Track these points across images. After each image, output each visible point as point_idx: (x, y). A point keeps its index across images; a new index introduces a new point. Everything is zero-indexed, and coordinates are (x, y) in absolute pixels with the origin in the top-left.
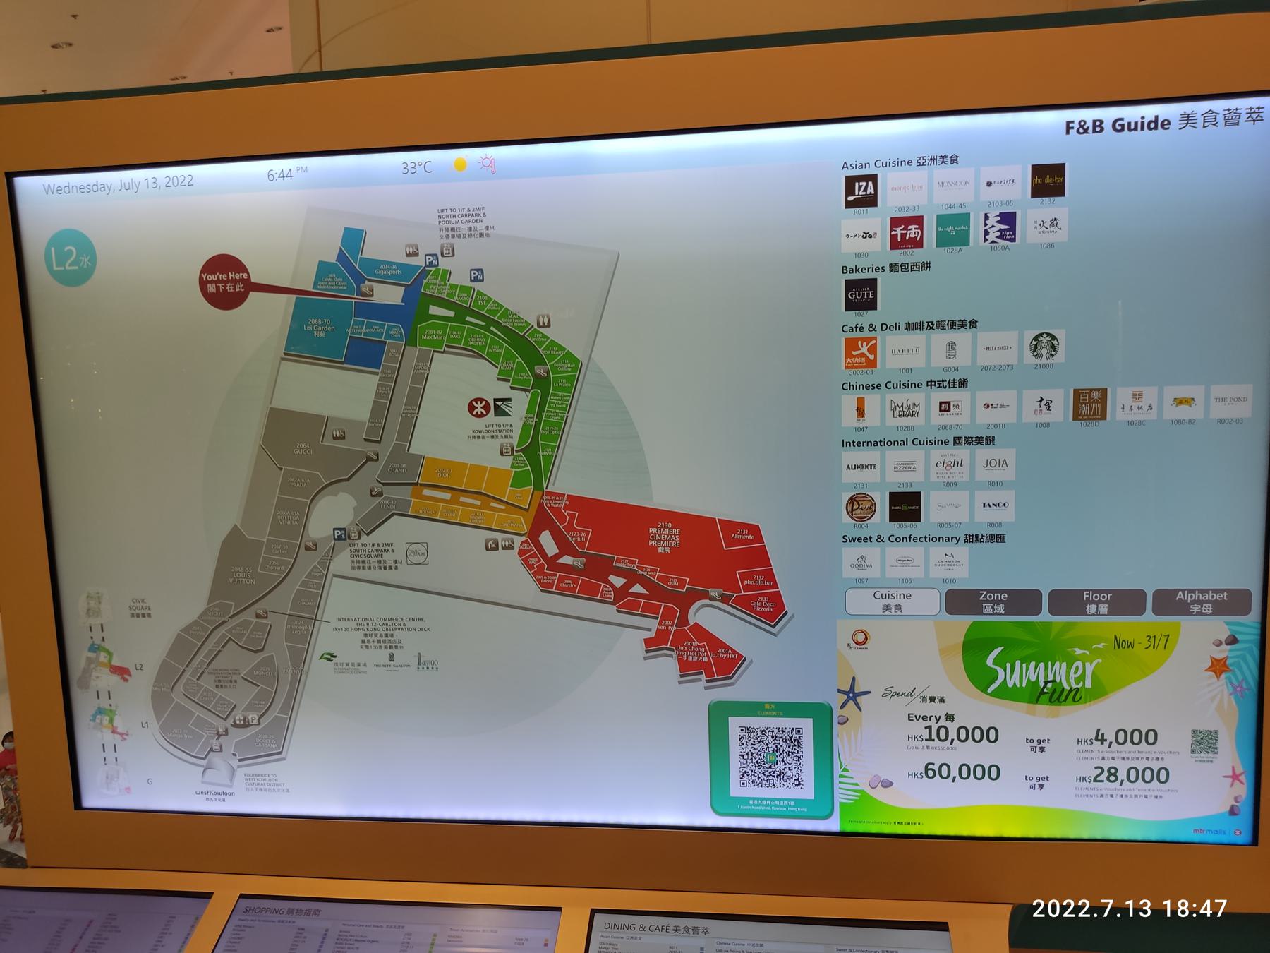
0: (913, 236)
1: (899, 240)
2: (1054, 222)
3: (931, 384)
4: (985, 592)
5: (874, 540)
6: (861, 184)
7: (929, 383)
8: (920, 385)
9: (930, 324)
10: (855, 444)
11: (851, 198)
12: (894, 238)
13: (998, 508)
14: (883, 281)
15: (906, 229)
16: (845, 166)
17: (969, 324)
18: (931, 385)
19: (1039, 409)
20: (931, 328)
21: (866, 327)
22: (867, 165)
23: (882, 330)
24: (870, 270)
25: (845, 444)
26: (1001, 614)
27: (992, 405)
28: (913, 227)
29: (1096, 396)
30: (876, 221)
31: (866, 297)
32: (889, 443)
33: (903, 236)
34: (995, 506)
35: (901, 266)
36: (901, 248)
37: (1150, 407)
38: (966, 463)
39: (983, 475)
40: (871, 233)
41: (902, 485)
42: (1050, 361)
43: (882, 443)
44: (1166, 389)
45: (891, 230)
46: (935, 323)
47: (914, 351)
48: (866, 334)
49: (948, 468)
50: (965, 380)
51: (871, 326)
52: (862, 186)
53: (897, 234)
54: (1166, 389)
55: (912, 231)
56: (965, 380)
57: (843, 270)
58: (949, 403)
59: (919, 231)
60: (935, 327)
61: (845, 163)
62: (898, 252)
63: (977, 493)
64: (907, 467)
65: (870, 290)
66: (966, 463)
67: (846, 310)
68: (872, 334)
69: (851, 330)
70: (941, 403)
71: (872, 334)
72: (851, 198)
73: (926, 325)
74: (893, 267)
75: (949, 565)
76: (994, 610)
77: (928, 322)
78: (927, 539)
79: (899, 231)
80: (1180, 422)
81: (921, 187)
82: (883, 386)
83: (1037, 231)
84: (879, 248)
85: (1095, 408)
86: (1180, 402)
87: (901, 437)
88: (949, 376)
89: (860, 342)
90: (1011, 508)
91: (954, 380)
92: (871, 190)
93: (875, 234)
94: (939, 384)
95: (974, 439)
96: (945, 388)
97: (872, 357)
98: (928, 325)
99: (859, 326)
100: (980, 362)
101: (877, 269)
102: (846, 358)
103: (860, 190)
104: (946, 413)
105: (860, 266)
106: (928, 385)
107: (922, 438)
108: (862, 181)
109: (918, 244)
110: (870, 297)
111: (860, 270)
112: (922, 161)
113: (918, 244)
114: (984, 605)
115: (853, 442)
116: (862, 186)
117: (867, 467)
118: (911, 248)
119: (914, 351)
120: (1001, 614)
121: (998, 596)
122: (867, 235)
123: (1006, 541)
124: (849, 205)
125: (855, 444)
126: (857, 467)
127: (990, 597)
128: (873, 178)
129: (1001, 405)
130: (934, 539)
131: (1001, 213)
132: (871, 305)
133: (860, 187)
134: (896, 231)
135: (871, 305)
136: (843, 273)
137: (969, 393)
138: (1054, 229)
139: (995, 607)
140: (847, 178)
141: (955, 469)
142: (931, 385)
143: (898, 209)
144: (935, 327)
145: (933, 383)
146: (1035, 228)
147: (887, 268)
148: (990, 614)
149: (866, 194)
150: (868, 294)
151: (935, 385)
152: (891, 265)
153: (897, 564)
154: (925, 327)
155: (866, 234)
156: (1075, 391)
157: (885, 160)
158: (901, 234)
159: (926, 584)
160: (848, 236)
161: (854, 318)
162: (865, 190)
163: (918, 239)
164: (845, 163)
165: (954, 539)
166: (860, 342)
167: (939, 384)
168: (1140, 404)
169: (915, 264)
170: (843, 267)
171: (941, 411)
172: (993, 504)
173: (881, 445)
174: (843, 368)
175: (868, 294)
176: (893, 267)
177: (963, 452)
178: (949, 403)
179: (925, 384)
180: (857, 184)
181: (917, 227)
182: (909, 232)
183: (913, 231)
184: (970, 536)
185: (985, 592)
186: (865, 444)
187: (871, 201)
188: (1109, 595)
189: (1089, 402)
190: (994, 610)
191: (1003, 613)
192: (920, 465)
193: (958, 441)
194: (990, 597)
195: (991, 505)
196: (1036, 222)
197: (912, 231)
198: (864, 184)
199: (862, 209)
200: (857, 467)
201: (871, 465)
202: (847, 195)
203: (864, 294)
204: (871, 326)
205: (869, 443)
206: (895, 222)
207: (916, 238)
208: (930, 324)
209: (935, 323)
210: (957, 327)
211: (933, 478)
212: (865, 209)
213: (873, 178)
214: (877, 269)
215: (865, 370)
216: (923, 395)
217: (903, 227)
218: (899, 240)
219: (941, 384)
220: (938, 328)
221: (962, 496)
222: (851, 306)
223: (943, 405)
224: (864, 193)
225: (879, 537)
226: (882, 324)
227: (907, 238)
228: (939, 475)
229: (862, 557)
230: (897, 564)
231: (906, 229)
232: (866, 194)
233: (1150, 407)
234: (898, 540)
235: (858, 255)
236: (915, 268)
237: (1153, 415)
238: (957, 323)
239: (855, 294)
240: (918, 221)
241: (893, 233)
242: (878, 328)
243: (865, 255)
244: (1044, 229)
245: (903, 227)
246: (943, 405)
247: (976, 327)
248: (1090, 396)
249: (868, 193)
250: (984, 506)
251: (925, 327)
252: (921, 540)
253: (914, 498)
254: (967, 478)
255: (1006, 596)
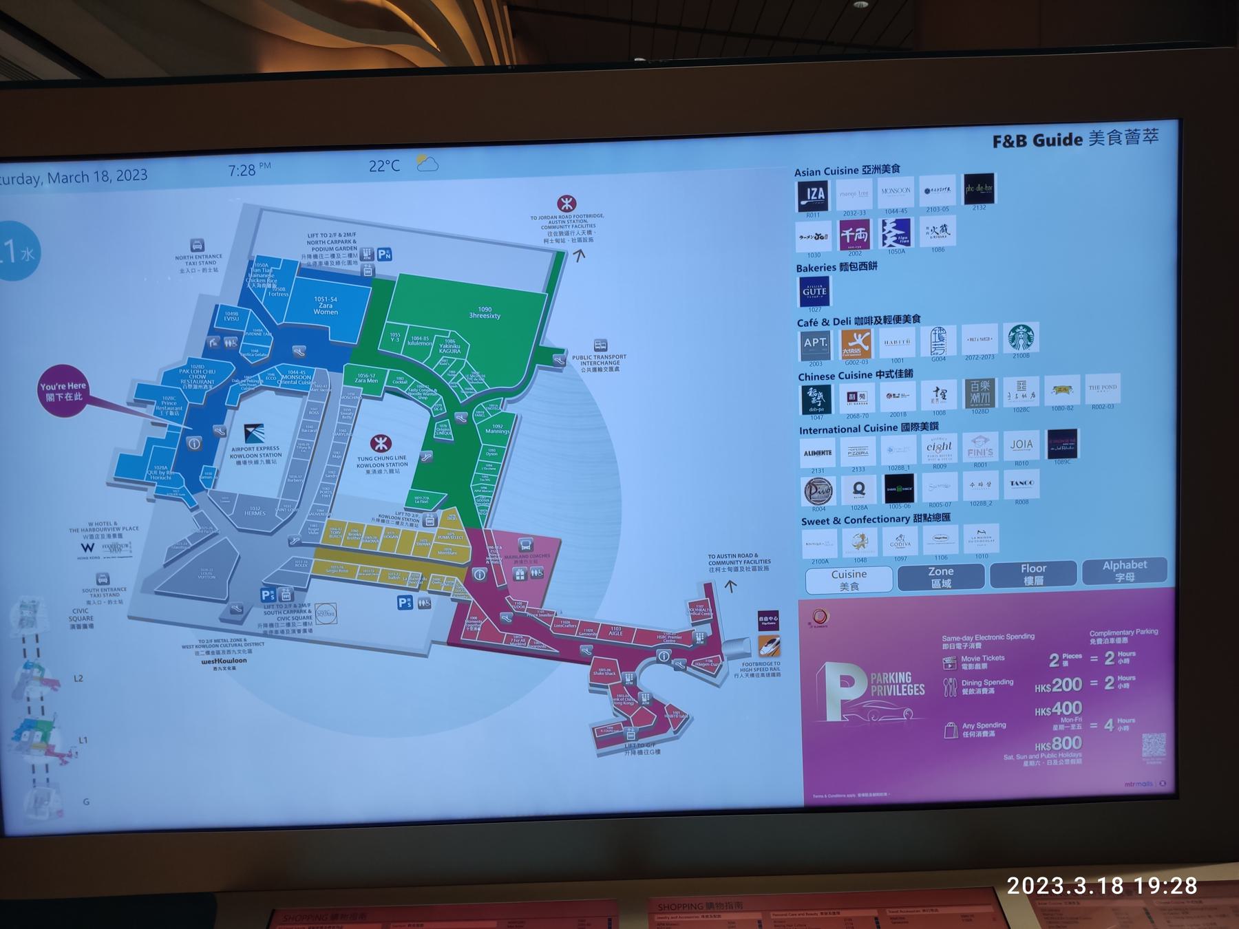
0: (860, 238)
1: (848, 241)
2: (944, 228)
3: (880, 374)
4: (933, 568)
5: (831, 521)
6: (813, 189)
7: (878, 374)
8: (870, 375)
9: (878, 318)
10: (812, 431)
11: (803, 203)
12: (843, 239)
13: (1024, 486)
14: (835, 279)
15: (854, 231)
16: (798, 173)
17: (912, 319)
18: (880, 375)
19: (935, 398)
20: (879, 323)
21: (820, 321)
22: (818, 173)
23: (835, 324)
24: (823, 269)
25: (802, 431)
26: (949, 589)
27: (894, 395)
28: (861, 229)
29: (985, 386)
30: (825, 224)
31: (819, 293)
32: (843, 430)
33: (852, 237)
34: (1023, 484)
35: (851, 265)
36: (850, 249)
37: (1033, 395)
38: (954, 446)
39: (1011, 456)
40: (823, 235)
41: (815, 471)
42: (1027, 351)
43: (837, 431)
44: (1047, 378)
45: (841, 232)
46: (882, 318)
47: (905, 342)
48: (820, 328)
49: (938, 451)
50: (911, 371)
51: (824, 320)
52: (813, 191)
53: (846, 236)
54: (1047, 378)
55: (860, 234)
56: (911, 371)
57: (798, 268)
58: (856, 393)
59: (866, 233)
60: (882, 322)
61: (798, 170)
62: (847, 252)
63: (965, 473)
64: (861, 452)
65: (823, 287)
66: (954, 446)
67: (801, 306)
68: (826, 328)
69: (806, 324)
70: (849, 394)
71: (826, 328)
72: (803, 203)
73: (874, 320)
74: (844, 267)
75: (981, 541)
76: (942, 585)
77: (876, 317)
78: (880, 520)
79: (847, 233)
80: (1059, 408)
81: (867, 193)
82: (837, 376)
83: (929, 236)
84: (829, 250)
85: (985, 397)
86: (1059, 390)
87: (853, 424)
88: (896, 367)
89: (855, 334)
90: (1037, 485)
91: (901, 370)
92: (821, 195)
93: (826, 235)
94: (888, 374)
95: (920, 425)
96: (893, 378)
97: (866, 348)
98: (876, 320)
99: (813, 321)
100: (965, 352)
101: (828, 268)
102: (843, 349)
103: (813, 195)
104: (853, 403)
105: (813, 265)
106: (877, 376)
107: (873, 425)
108: (814, 187)
109: (865, 245)
110: (823, 293)
111: (813, 269)
112: (867, 170)
113: (865, 245)
114: (933, 580)
115: (810, 429)
116: (813, 191)
117: (823, 453)
118: (859, 249)
119: (905, 342)
120: (949, 589)
121: (945, 572)
122: (819, 237)
123: (951, 519)
124: (802, 209)
125: (812, 431)
126: (814, 453)
127: (938, 572)
128: (823, 185)
129: (902, 395)
130: (886, 520)
131: (897, 220)
132: (824, 301)
133: (812, 192)
134: (845, 233)
135: (824, 301)
136: (798, 271)
137: (915, 382)
138: (945, 234)
139: (943, 582)
140: (800, 184)
141: (945, 452)
142: (880, 375)
143: (846, 213)
144: (882, 322)
145: (882, 374)
146: (928, 233)
147: (838, 267)
148: (939, 589)
149: (818, 199)
150: (821, 291)
151: (883, 375)
152: (841, 265)
153: (934, 542)
154: (874, 321)
155: (818, 235)
156: (967, 381)
157: (834, 168)
158: (850, 236)
159: (879, 561)
160: (802, 237)
161: (809, 313)
162: (817, 195)
163: (865, 240)
164: (798, 170)
165: (905, 519)
166: (855, 334)
167: (888, 374)
168: (1024, 393)
169: (863, 264)
170: (798, 266)
171: (849, 400)
172: (1021, 483)
173: (836, 432)
174: (840, 358)
175: (821, 291)
176: (844, 267)
177: (911, 437)
178: (856, 393)
179: (874, 374)
180: (809, 190)
181: (864, 229)
182: (857, 234)
183: (861, 233)
184: (918, 515)
185: (933, 568)
186: (821, 431)
187: (822, 206)
188: (1044, 567)
189: (980, 392)
190: (942, 585)
191: (950, 587)
192: (872, 450)
193: (906, 427)
194: (938, 572)
195: (1019, 483)
196: (928, 228)
197: (860, 234)
198: (815, 190)
199: (814, 212)
200: (814, 453)
201: (827, 451)
202: (801, 198)
203: (817, 291)
204: (824, 320)
205: (825, 431)
206: (845, 225)
207: (863, 239)
208: (878, 318)
209: (882, 318)
210: (902, 322)
211: (925, 461)
212: (817, 212)
213: (823, 185)
214: (828, 268)
215: (860, 360)
216: (873, 385)
217: (851, 229)
218: (848, 241)
219: (889, 374)
220: (885, 322)
221: (950, 477)
222: (805, 302)
223: (851, 395)
224: (816, 198)
225: (836, 519)
226: (835, 319)
227: (855, 240)
228: (929, 458)
229: (901, 536)
230: (934, 542)
231: (854, 231)
232: (818, 199)
233: (1033, 395)
234: (854, 521)
235: (811, 255)
236: (863, 268)
237: (1035, 403)
238: (902, 318)
239: (809, 291)
240: (865, 224)
241: (843, 235)
242: (831, 323)
243: (818, 255)
244: (935, 234)
245: (851, 229)
246: (851, 395)
247: (919, 322)
248: (980, 385)
249: (819, 198)
250: (1012, 484)
251: (874, 321)
252: (875, 520)
253: (907, 480)
254: (955, 460)
255: (953, 571)
